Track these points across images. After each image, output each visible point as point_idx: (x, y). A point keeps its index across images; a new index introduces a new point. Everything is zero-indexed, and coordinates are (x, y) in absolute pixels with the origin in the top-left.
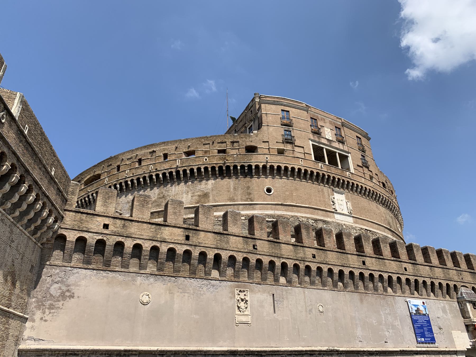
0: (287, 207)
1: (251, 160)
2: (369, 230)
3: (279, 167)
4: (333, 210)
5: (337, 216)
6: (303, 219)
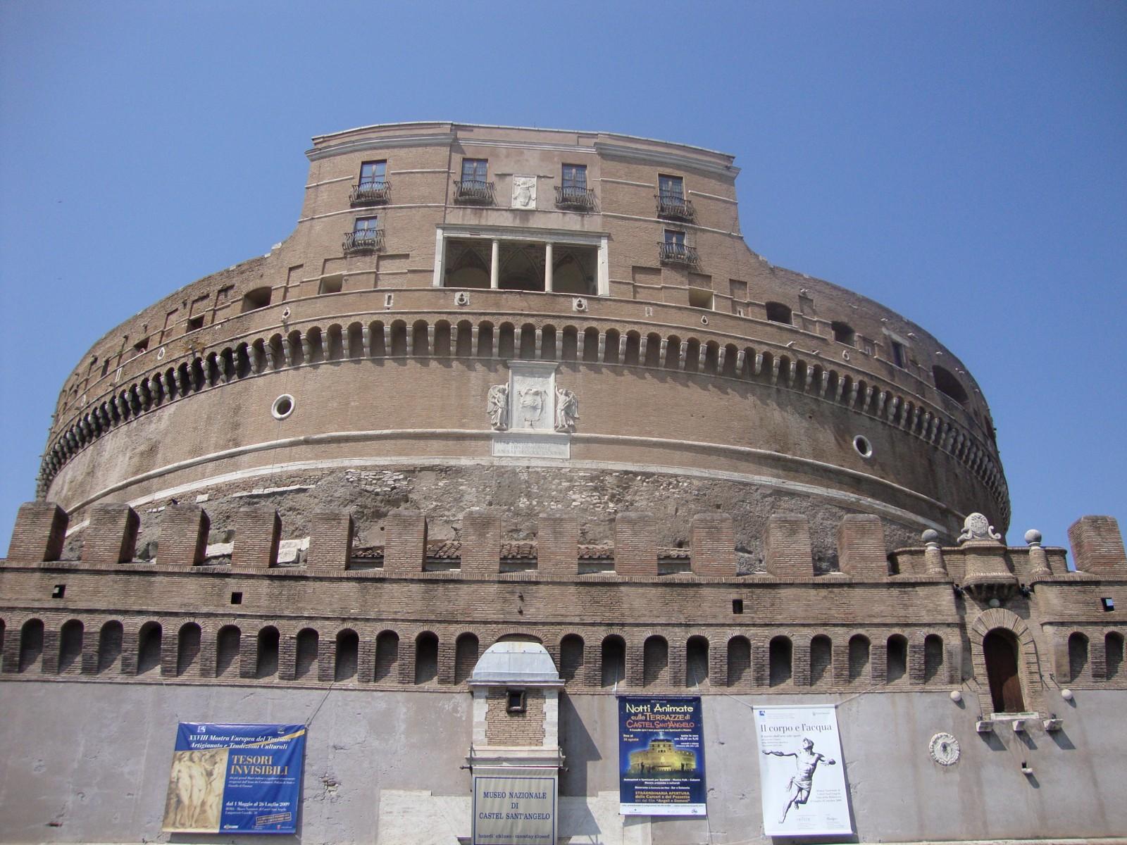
0: (323, 447)
1: (248, 329)
2: (643, 474)
4: (493, 430)
5: (499, 448)
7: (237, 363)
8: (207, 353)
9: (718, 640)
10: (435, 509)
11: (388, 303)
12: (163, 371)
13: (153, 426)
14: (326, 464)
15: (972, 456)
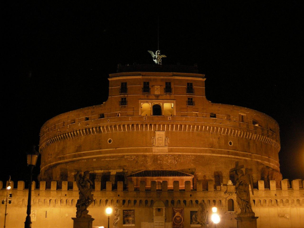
5: (153, 151)
8: (91, 127)
9: (188, 200)
12: (81, 129)
14: (119, 154)
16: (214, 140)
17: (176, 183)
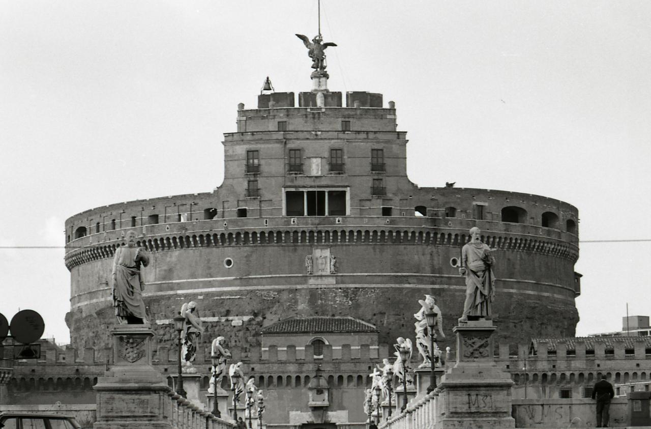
2: (362, 288)
3: (238, 234)
5: (312, 281)
6: (263, 293)
7: (207, 240)
8: (191, 235)
10: (289, 305)
11: (266, 223)
12: (171, 237)
13: (168, 259)
14: (249, 288)
15: (522, 245)
16: (423, 258)
17: (346, 346)
